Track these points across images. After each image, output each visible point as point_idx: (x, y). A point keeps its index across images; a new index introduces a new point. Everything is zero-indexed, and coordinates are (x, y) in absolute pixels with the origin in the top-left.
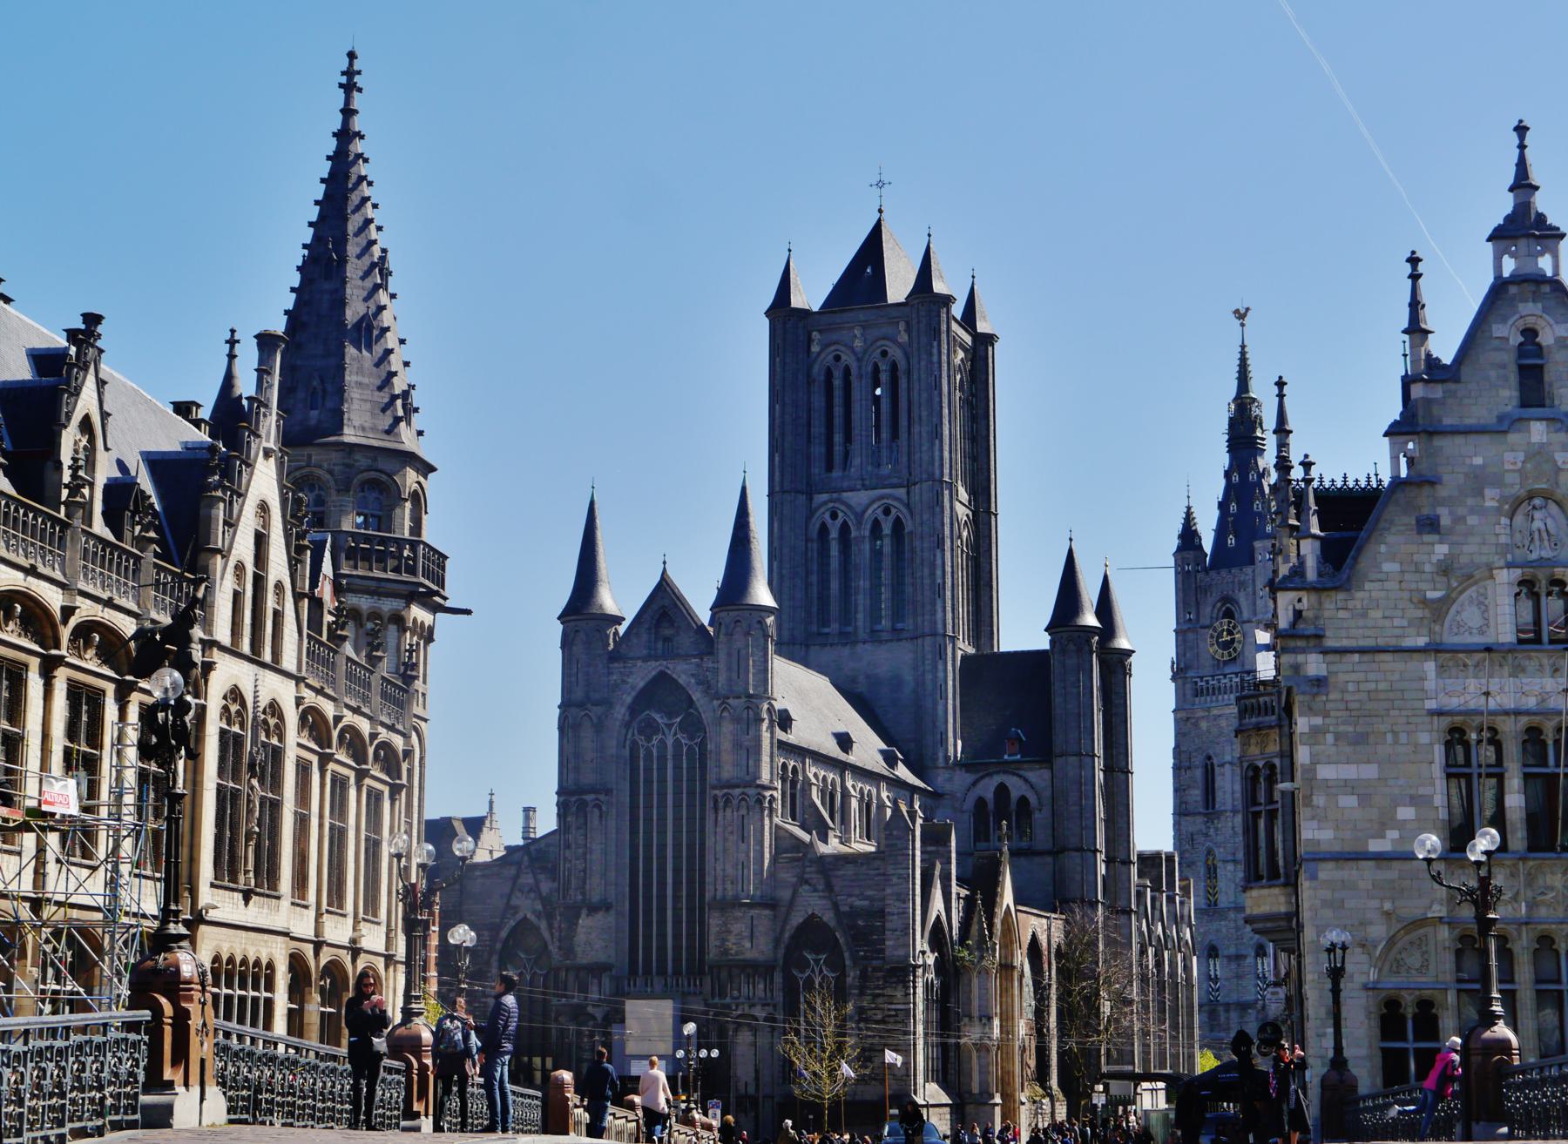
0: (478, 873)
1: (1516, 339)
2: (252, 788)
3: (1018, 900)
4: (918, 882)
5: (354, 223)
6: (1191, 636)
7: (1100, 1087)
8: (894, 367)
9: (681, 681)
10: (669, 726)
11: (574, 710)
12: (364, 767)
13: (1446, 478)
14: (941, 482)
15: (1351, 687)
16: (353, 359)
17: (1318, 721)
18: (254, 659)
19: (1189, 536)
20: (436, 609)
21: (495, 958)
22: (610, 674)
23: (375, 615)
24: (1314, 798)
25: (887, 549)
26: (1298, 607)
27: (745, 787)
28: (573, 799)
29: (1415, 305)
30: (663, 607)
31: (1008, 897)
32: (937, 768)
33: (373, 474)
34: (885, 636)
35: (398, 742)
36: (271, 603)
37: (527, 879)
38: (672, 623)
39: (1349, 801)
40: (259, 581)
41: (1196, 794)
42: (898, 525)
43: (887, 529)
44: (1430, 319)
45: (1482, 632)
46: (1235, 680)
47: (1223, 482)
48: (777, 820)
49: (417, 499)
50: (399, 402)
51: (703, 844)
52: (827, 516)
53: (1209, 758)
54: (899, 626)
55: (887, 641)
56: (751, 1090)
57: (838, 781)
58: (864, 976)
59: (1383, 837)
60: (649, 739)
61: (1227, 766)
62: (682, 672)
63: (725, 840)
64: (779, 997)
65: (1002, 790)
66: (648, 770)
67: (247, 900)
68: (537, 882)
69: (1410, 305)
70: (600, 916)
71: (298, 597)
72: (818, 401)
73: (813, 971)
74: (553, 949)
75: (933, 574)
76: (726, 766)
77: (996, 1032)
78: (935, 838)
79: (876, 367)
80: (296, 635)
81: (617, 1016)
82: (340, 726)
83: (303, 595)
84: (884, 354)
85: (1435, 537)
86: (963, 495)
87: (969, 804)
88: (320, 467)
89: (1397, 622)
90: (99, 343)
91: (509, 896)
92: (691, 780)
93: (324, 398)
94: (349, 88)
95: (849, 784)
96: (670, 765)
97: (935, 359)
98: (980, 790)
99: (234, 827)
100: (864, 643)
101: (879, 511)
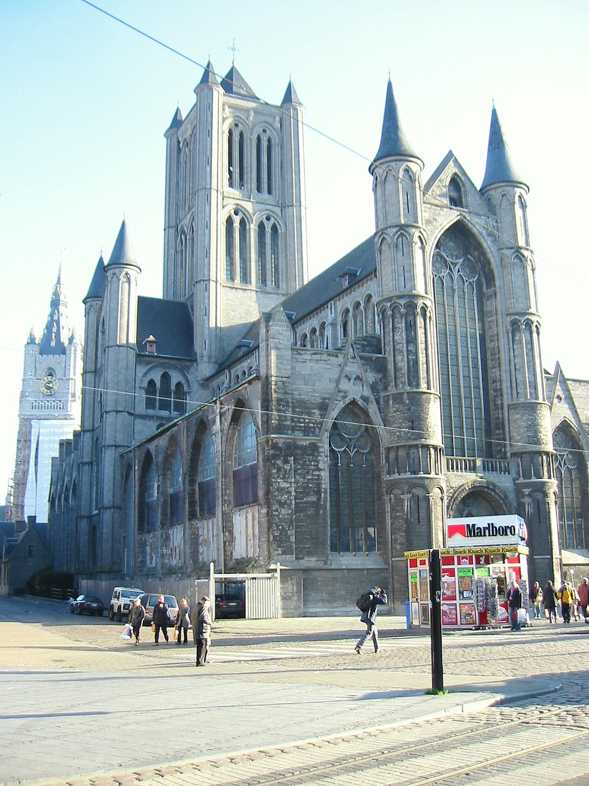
9: (475, 230)
21: (327, 434)
37: (354, 368)
42: (274, 228)
43: (268, 229)
46: (53, 403)
52: (233, 212)
55: (271, 293)
73: (560, 464)
84: (264, 131)
91: (338, 382)
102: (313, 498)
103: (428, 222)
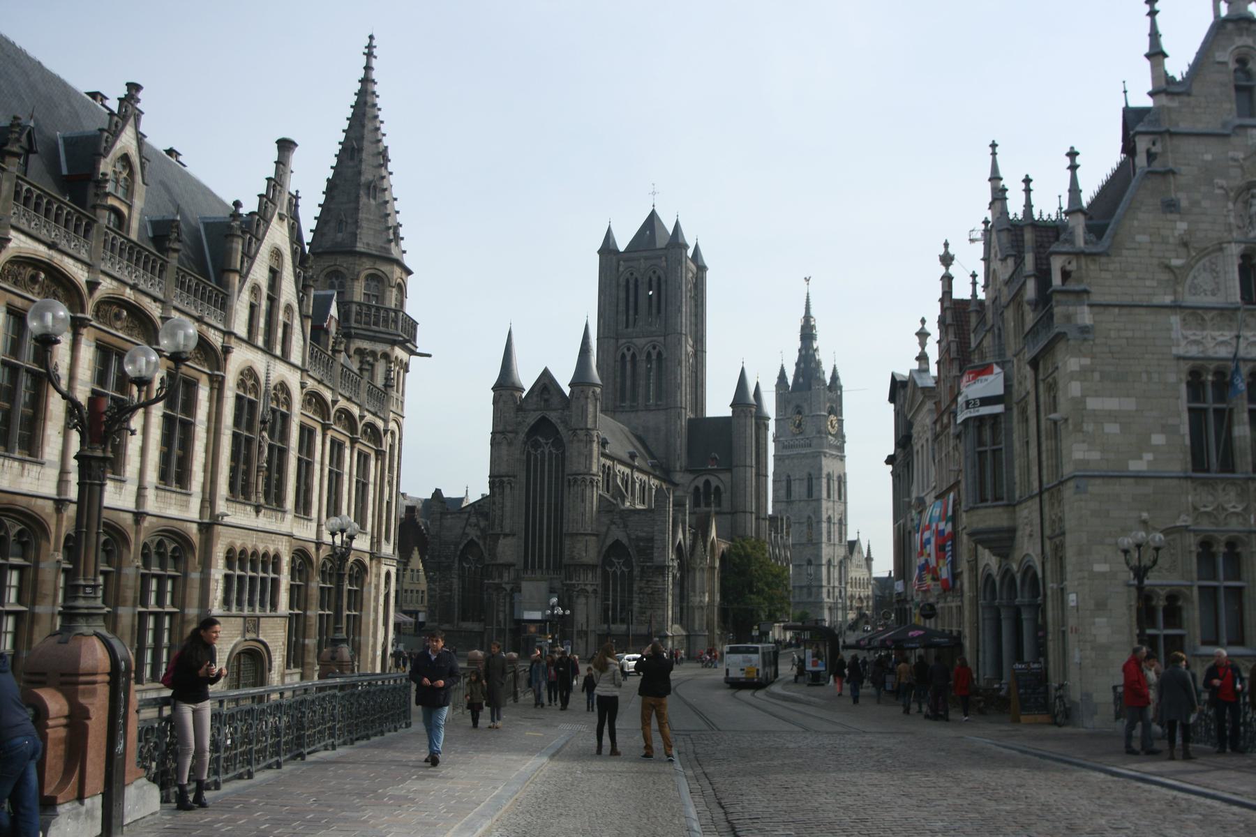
0: (449, 516)
1: (1232, 66)
2: (263, 437)
3: (718, 536)
4: (671, 524)
5: (369, 126)
6: (782, 422)
7: (756, 627)
8: (659, 279)
9: (553, 421)
10: (547, 444)
11: (498, 436)
12: (355, 436)
13: (1184, 169)
14: (681, 334)
15: (1113, 334)
16: (364, 204)
17: (1086, 361)
18: (268, 350)
19: (782, 376)
20: (412, 353)
21: (457, 559)
22: (517, 417)
23: (373, 354)
24: (1085, 426)
25: (654, 366)
26: (1069, 268)
27: (585, 474)
28: (497, 480)
29: (1154, 35)
30: (545, 384)
31: (713, 534)
32: (676, 471)
33: (372, 271)
34: (652, 408)
35: (380, 424)
36: (281, 317)
37: (473, 520)
38: (549, 393)
39: (1112, 428)
40: (272, 300)
41: (783, 492)
42: (659, 354)
43: (654, 357)
44: (1166, 45)
45: (1214, 294)
47: (798, 354)
48: (601, 492)
49: (401, 288)
50: (391, 231)
51: (562, 504)
52: (625, 350)
53: (789, 476)
54: (659, 403)
56: (584, 628)
57: (630, 473)
58: (642, 571)
59: (1141, 458)
60: (536, 451)
61: (797, 482)
62: (553, 416)
63: (574, 501)
64: (599, 581)
65: (707, 483)
66: (535, 465)
67: (257, 512)
68: (478, 521)
69: (1150, 35)
70: (510, 538)
71: (303, 317)
72: (622, 295)
74: (486, 555)
75: (675, 378)
76: (575, 465)
77: (707, 599)
78: (679, 504)
79: (650, 280)
80: (302, 343)
81: (517, 589)
82: (336, 407)
83: (307, 317)
84: (654, 272)
85: (1176, 216)
86: (690, 342)
87: (691, 489)
88: (342, 266)
89: (1148, 283)
90: (139, 106)
91: (465, 528)
92: (557, 471)
93: (346, 226)
94: (369, 55)
95: (635, 477)
96: (546, 464)
97: (679, 275)
98: (696, 483)
99: (248, 461)
100: (642, 411)
101: (651, 348)
102: (449, 593)
103: (519, 424)
